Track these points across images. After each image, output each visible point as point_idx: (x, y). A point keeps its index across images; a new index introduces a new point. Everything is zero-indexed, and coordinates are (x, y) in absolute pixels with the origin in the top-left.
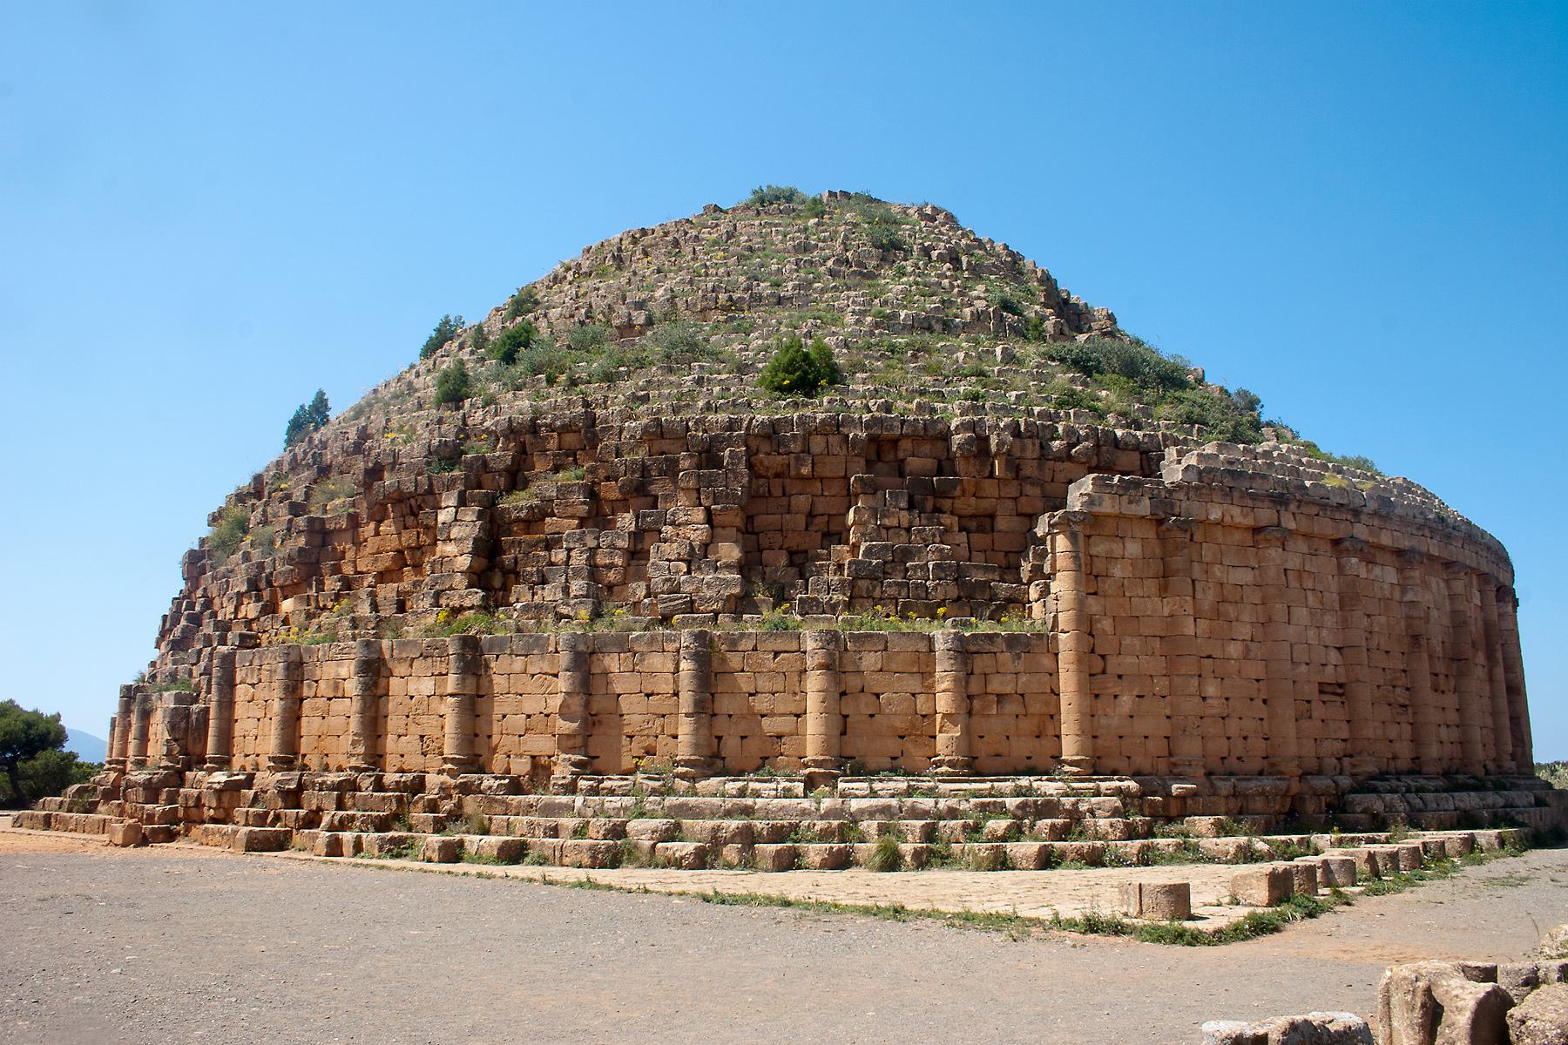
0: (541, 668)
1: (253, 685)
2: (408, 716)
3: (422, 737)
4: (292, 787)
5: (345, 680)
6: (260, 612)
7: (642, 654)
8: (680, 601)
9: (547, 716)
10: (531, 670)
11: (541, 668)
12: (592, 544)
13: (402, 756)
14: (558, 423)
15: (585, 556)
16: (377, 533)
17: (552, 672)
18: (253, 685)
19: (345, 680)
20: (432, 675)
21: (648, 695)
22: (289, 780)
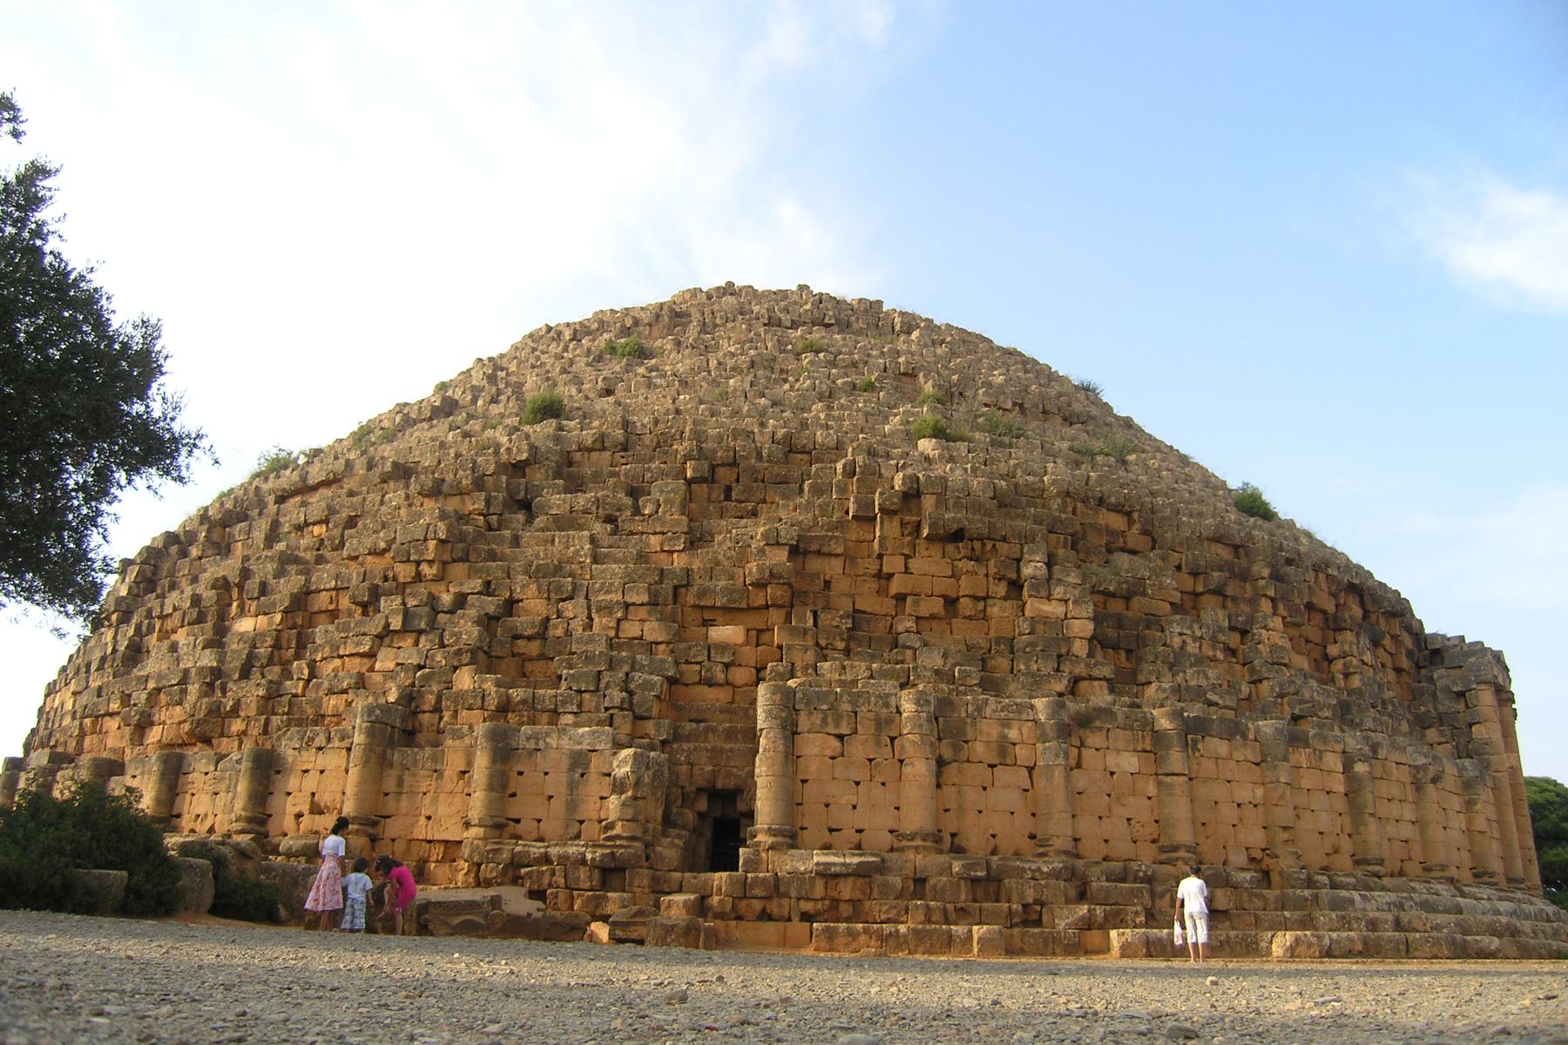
0: (1245, 756)
1: (841, 737)
2: (1109, 795)
3: (1129, 820)
4: (979, 874)
5: (1014, 744)
6: (674, 635)
7: (1320, 752)
8: (1309, 705)
9: (1255, 806)
10: (1238, 755)
11: (1245, 756)
12: (1198, 634)
13: (1106, 841)
14: (1113, 500)
15: (1198, 644)
16: (907, 572)
17: (1253, 760)
18: (841, 737)
19: (1014, 744)
20: (1135, 751)
21: (1328, 793)
22: (975, 864)
